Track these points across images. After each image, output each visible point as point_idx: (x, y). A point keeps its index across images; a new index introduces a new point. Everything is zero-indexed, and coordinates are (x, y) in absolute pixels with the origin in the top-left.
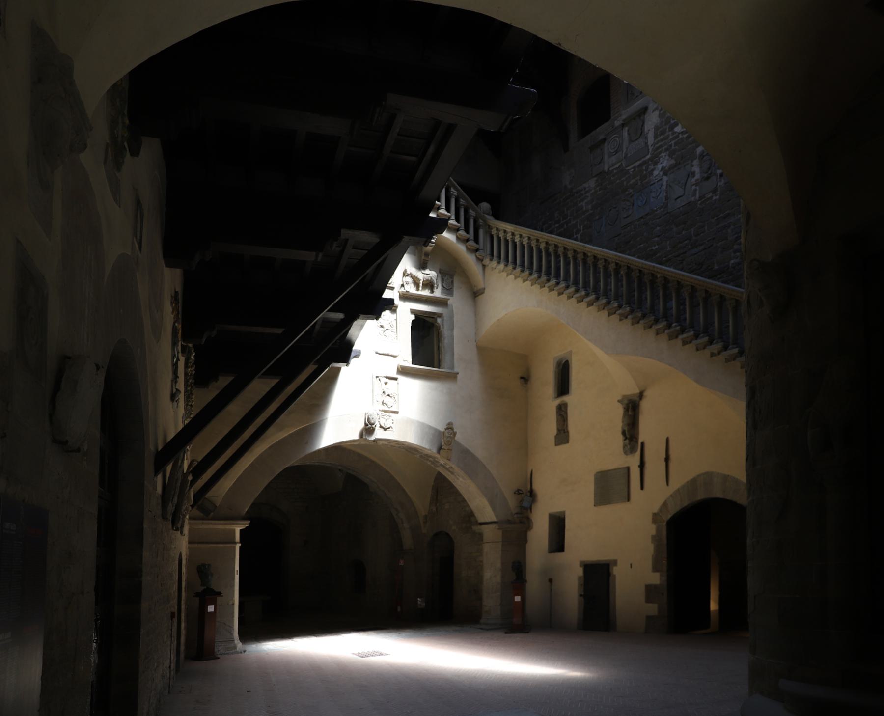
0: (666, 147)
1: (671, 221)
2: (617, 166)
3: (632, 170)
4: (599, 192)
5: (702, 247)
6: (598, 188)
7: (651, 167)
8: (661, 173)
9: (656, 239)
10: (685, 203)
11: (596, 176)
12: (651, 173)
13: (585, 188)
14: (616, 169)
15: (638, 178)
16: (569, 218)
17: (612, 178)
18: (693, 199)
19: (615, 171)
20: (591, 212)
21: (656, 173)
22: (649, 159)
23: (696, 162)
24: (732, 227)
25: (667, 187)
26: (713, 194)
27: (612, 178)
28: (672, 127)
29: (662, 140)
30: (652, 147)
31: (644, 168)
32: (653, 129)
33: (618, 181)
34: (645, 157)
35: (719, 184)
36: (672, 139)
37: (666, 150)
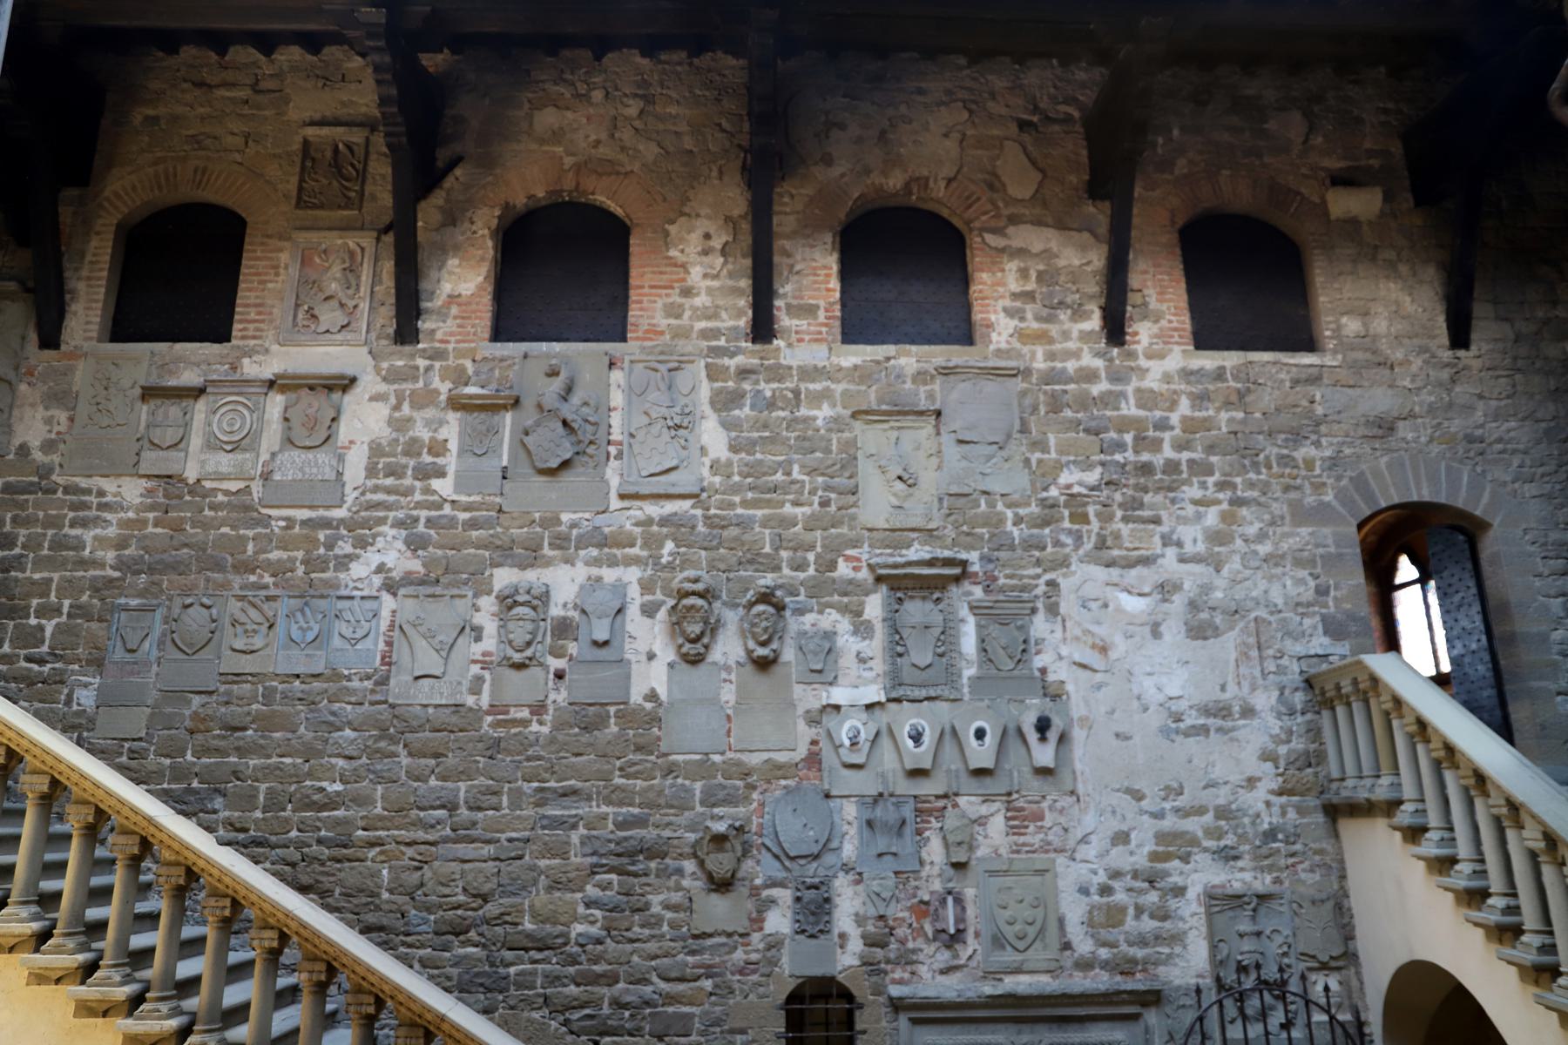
0: (401, 514)
1: (392, 730)
2: (234, 486)
3: (283, 524)
4: (150, 529)
5: (489, 850)
6: (151, 515)
7: (345, 547)
8: (377, 580)
9: (341, 762)
10: (444, 702)
11: (148, 477)
12: (344, 562)
13: (101, 493)
14: (227, 493)
15: (300, 554)
16: (17, 551)
17: (207, 512)
18: (470, 701)
19: (220, 498)
20: (117, 574)
21: (358, 570)
22: (342, 521)
23: (488, 603)
24: (582, 831)
25: (392, 627)
26: (532, 713)
27: (207, 512)
28: (425, 473)
29: (388, 491)
30: (356, 494)
31: (321, 536)
32: (366, 447)
33: (225, 530)
34: (328, 507)
35: (552, 696)
36: (419, 505)
37: (399, 524)
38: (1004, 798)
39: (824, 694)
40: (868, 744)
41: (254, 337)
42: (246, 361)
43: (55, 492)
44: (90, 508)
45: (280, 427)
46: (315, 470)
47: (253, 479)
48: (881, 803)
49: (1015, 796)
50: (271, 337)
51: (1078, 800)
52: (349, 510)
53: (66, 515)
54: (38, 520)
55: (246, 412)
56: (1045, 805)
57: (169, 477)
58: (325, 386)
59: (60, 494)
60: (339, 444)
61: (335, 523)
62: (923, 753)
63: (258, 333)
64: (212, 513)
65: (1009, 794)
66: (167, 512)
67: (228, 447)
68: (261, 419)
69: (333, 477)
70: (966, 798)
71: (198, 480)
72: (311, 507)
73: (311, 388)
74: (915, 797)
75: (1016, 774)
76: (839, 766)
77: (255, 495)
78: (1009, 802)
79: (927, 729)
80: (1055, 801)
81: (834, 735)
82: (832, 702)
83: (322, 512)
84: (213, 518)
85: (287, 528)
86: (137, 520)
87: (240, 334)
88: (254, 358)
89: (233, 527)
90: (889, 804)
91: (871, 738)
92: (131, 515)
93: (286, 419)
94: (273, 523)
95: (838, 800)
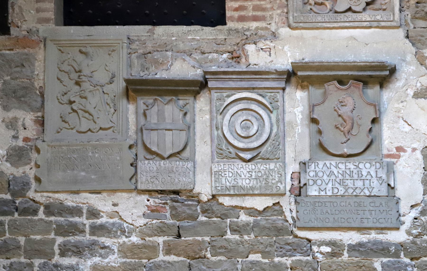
3: (328, 249)
4: (162, 257)
6: (160, 240)
11: (149, 192)
14: (251, 211)
17: (229, 236)
19: (244, 218)
27: (229, 236)
30: (414, 213)
33: (254, 257)
34: (382, 229)
41: (255, 19)
42: (250, 48)
43: (35, 212)
44: (83, 232)
45: (307, 131)
46: (359, 184)
47: (283, 195)
50: (276, 18)
52: (409, 233)
53: (53, 241)
54: (19, 247)
55: (262, 112)
57: (176, 192)
58: (358, 79)
59: (41, 215)
60: (385, 152)
61: (393, 249)
63: (259, 13)
64: (237, 237)
66: (179, 236)
67: (247, 156)
68: (281, 120)
69: (384, 191)
71: (214, 196)
72: (359, 229)
73: (341, 81)
77: (288, 215)
83: (373, 236)
84: (237, 243)
85: (333, 254)
86: (145, 246)
87: (236, 14)
88: (261, 45)
89: (265, 254)
92: (135, 239)
93: (314, 121)
94: (315, 248)
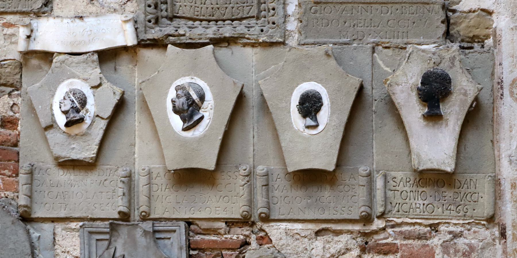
38: (357, 227)
39: (23, 32)
40: (102, 124)
48: (124, 231)
49: (378, 224)
51: (503, 235)
56: (436, 241)
62: (200, 140)
65: (367, 219)
70: (283, 225)
74: (189, 223)
75: (379, 183)
76: (51, 164)
78: (365, 234)
79: (209, 96)
80: (456, 236)
81: (39, 108)
82: (37, 46)
90: (139, 233)
91: (108, 112)
95: (47, 227)
